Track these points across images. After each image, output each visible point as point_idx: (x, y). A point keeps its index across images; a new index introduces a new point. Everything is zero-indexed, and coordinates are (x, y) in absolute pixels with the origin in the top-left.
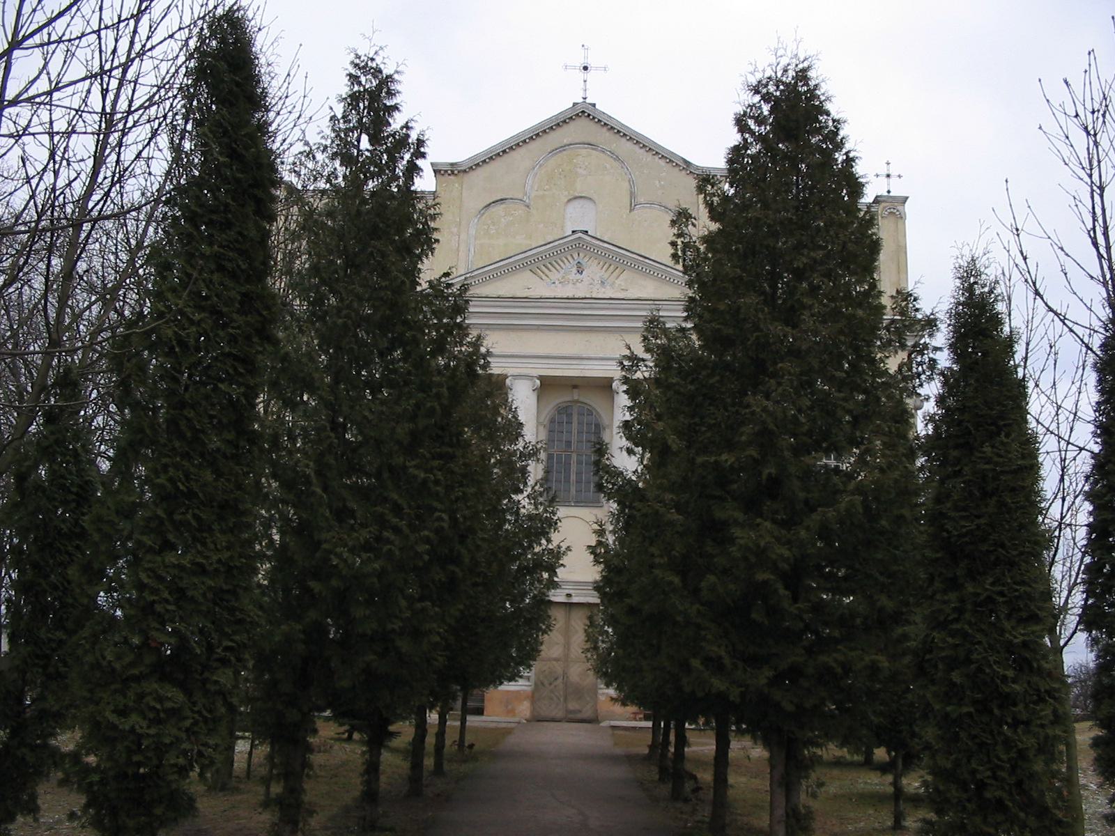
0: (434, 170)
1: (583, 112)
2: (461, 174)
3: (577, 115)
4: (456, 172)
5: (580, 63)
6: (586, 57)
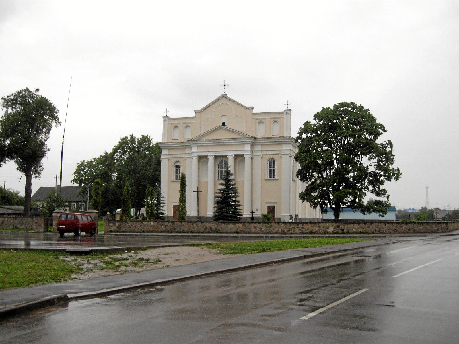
5: (223, 84)
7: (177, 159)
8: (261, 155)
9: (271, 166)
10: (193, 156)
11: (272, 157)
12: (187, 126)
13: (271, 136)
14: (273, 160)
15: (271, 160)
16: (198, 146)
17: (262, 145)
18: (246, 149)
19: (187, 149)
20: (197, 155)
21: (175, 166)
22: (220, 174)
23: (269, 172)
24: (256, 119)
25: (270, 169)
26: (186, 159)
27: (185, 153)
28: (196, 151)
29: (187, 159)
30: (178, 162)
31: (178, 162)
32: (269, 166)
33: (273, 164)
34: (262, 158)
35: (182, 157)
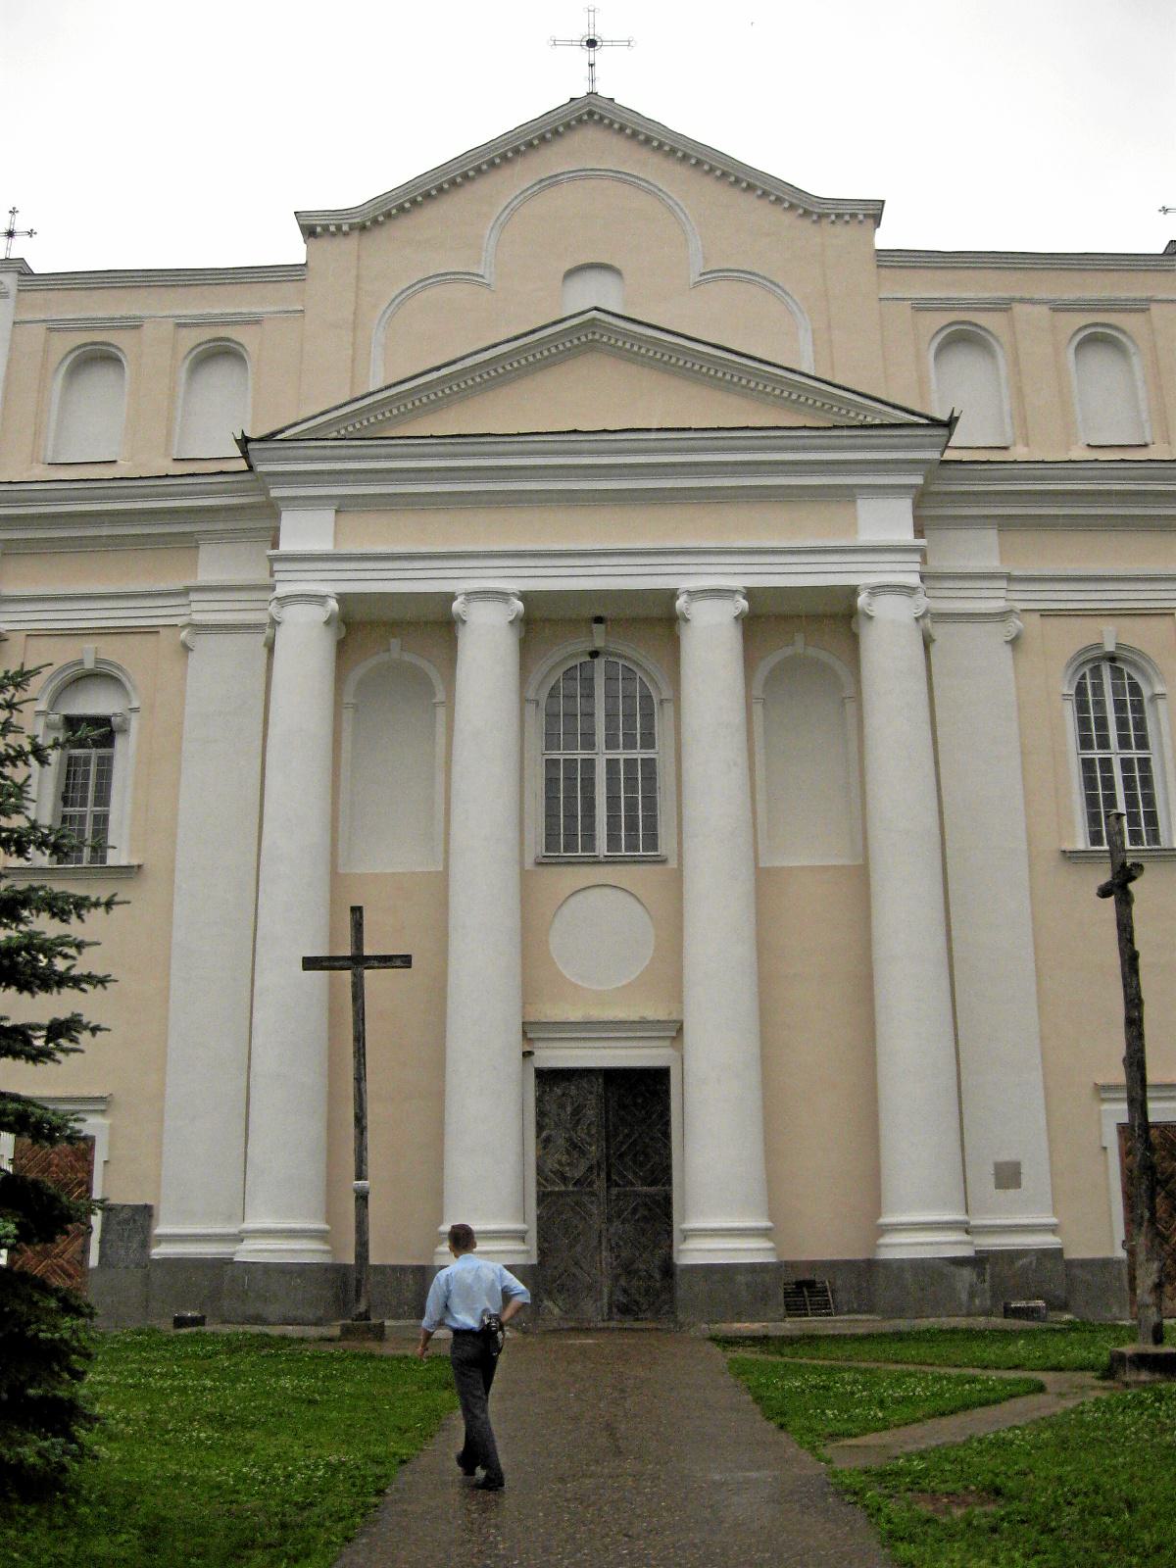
0: (302, 227)
1: (591, 114)
2: (356, 234)
3: (580, 120)
4: (345, 228)
5: (582, 32)
6: (592, 25)
7: (88, 653)
8: (1002, 616)
9: (1102, 723)
10: (284, 601)
11: (1109, 635)
12: (220, 353)
13: (1079, 453)
14: (1117, 673)
15: (1096, 672)
16: (343, 507)
17: (1005, 524)
18: (865, 538)
19: (206, 552)
20: (330, 584)
21: (56, 718)
22: (570, 799)
23: (1089, 783)
24: (921, 306)
25: (1096, 754)
26: (186, 648)
27: (178, 584)
28: (326, 546)
29: (205, 644)
30: (101, 676)
31: (101, 676)
32: (1083, 723)
33: (1120, 706)
34: (1014, 642)
35: (152, 631)
